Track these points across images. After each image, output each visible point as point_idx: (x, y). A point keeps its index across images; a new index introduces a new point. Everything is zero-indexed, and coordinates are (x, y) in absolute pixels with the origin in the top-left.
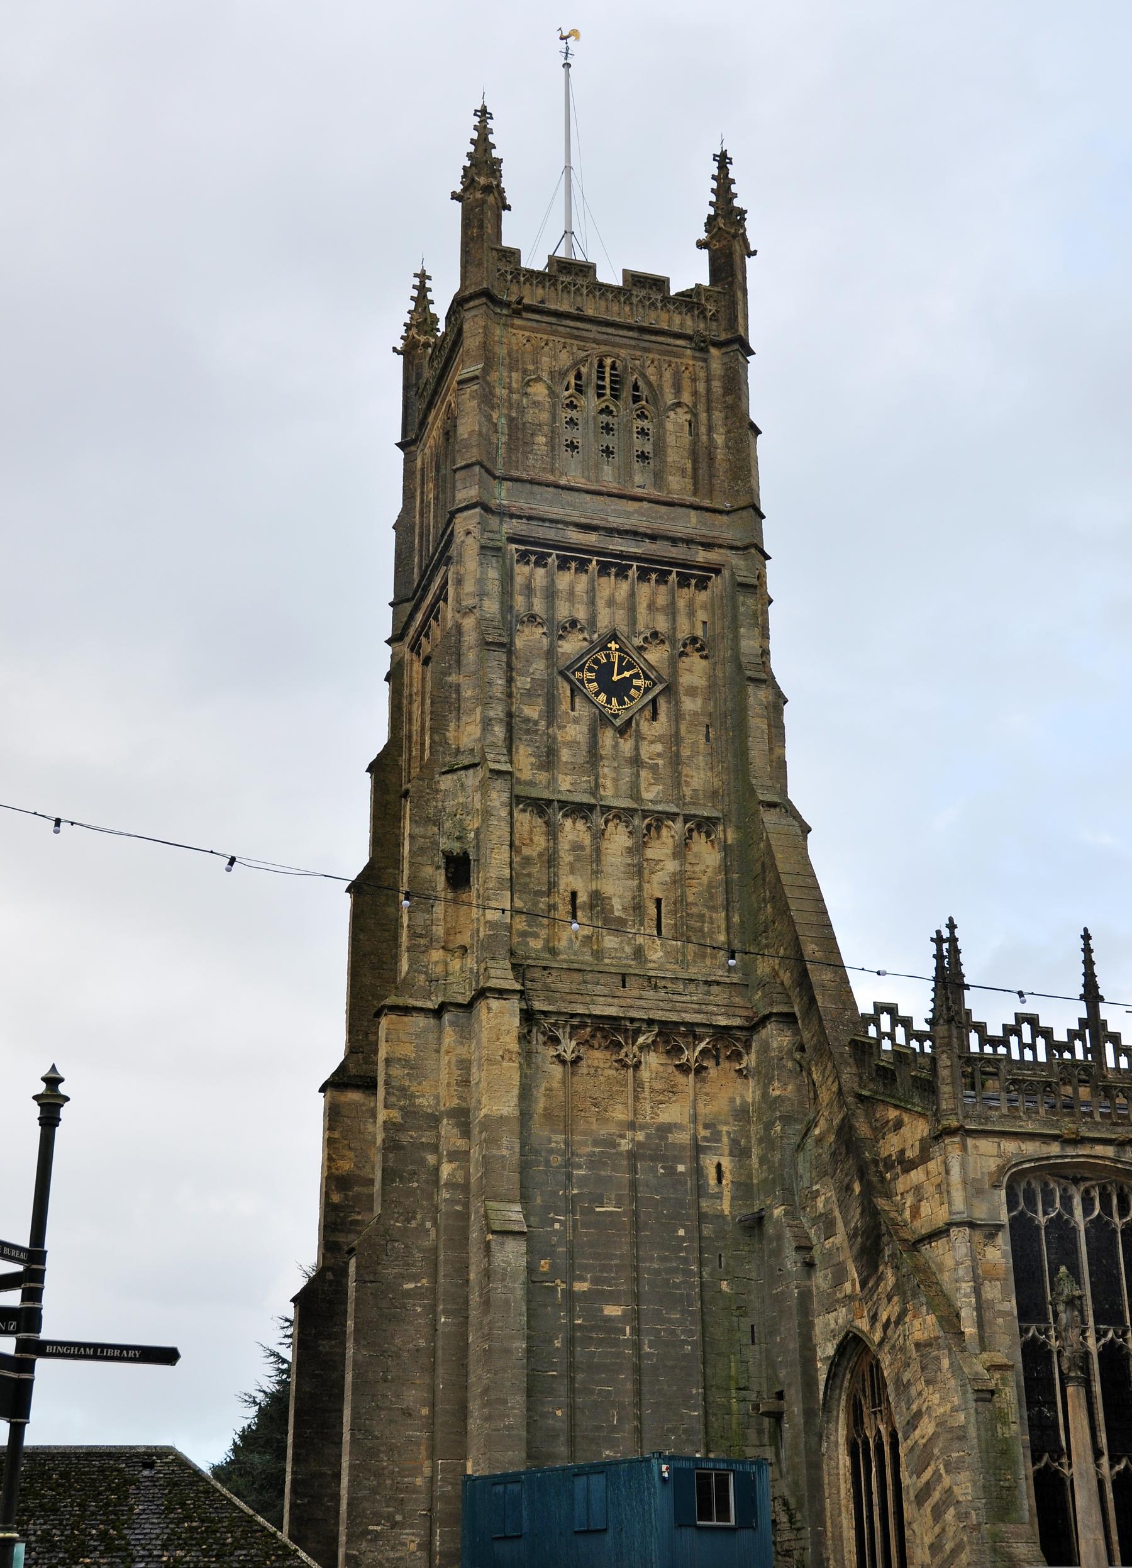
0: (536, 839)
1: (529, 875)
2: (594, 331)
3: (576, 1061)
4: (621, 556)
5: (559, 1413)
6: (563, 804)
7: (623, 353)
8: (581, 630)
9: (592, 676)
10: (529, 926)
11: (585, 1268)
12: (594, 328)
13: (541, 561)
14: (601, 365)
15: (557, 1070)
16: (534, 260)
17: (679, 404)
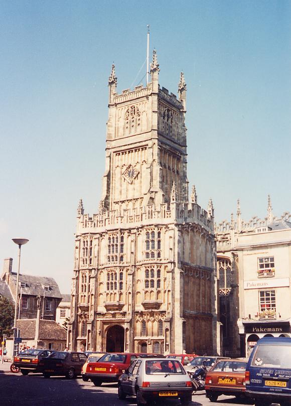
2: (129, 103)
6: (121, 202)
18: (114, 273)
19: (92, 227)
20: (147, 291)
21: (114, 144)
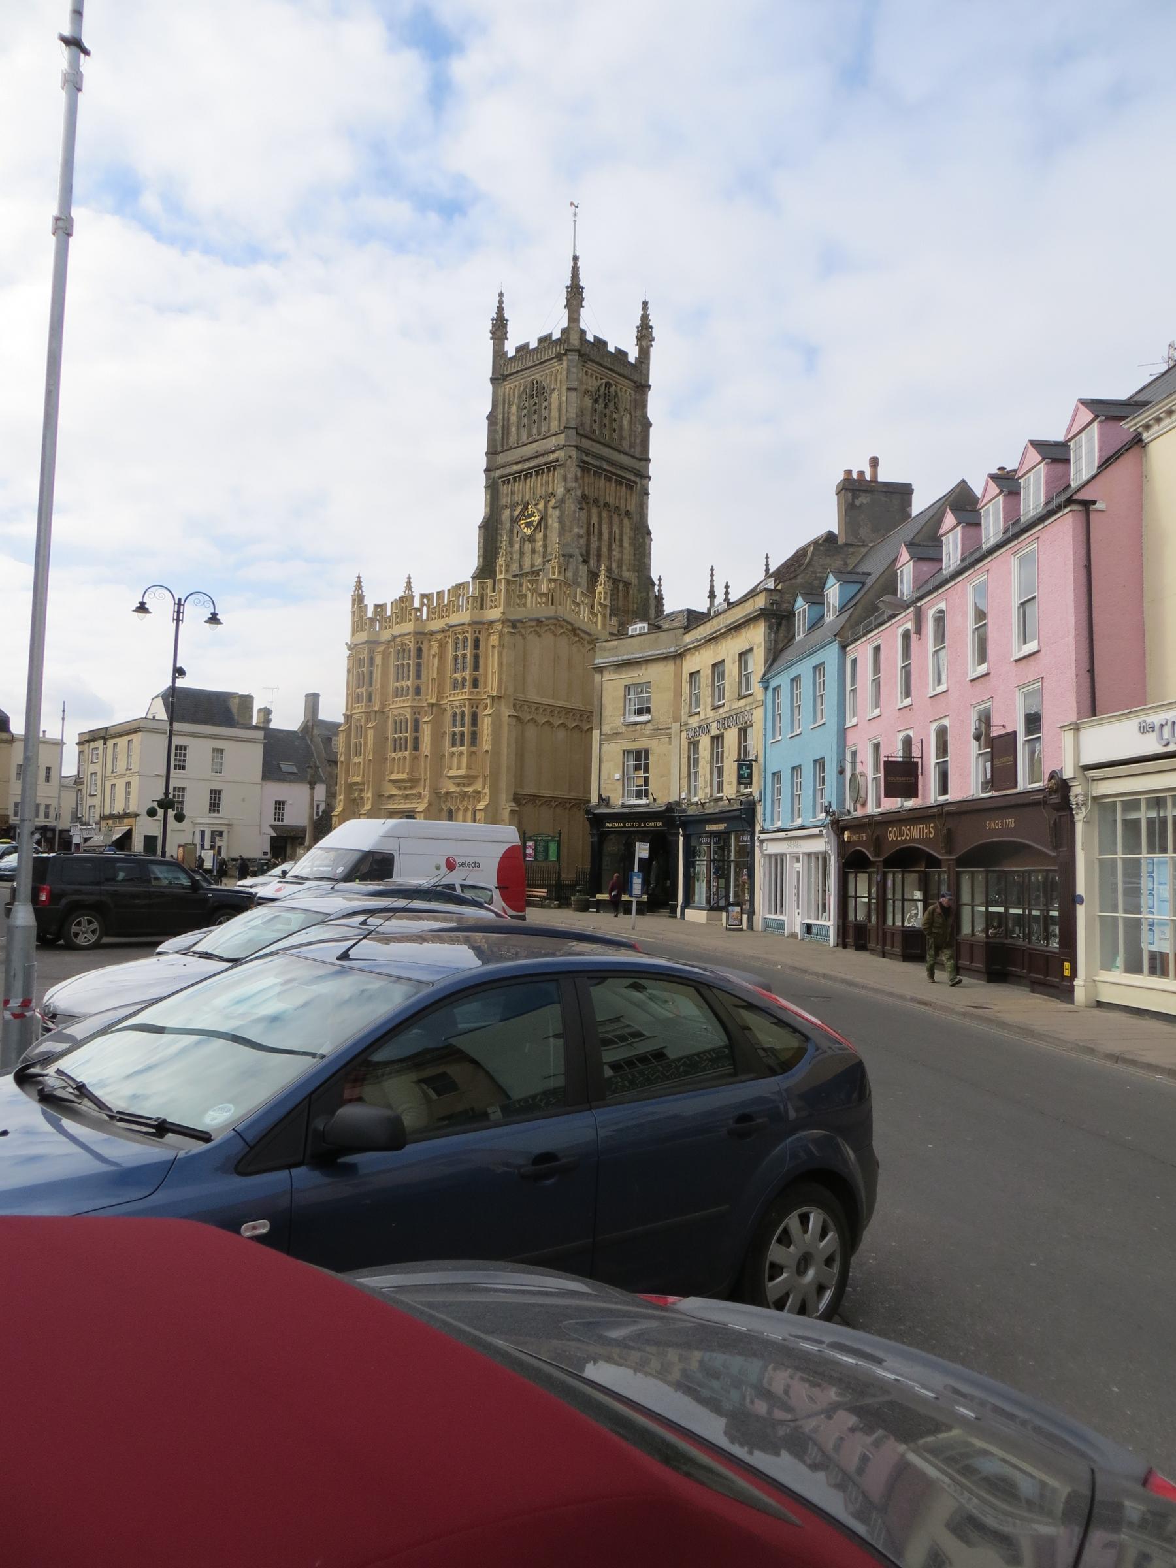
4: (529, 469)
7: (536, 376)
16: (511, 353)
17: (554, 389)
20: (453, 754)
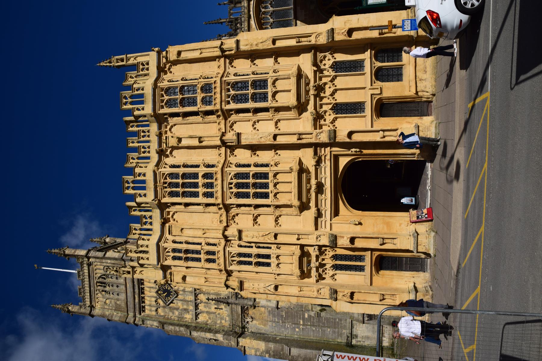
0: (204, 316)
1: (213, 318)
3: (252, 318)
5: (329, 330)
6: (196, 310)
8: (157, 299)
9: (167, 298)
10: (224, 319)
11: (297, 321)
12: (92, 288)
13: (144, 307)
14: (99, 286)
15: (254, 322)
18: (235, 181)
19: (149, 240)
21: (131, 314)
